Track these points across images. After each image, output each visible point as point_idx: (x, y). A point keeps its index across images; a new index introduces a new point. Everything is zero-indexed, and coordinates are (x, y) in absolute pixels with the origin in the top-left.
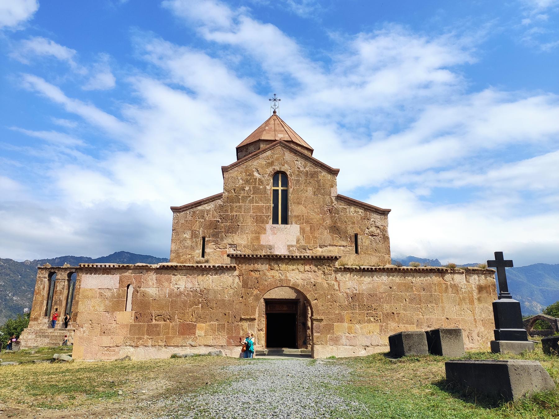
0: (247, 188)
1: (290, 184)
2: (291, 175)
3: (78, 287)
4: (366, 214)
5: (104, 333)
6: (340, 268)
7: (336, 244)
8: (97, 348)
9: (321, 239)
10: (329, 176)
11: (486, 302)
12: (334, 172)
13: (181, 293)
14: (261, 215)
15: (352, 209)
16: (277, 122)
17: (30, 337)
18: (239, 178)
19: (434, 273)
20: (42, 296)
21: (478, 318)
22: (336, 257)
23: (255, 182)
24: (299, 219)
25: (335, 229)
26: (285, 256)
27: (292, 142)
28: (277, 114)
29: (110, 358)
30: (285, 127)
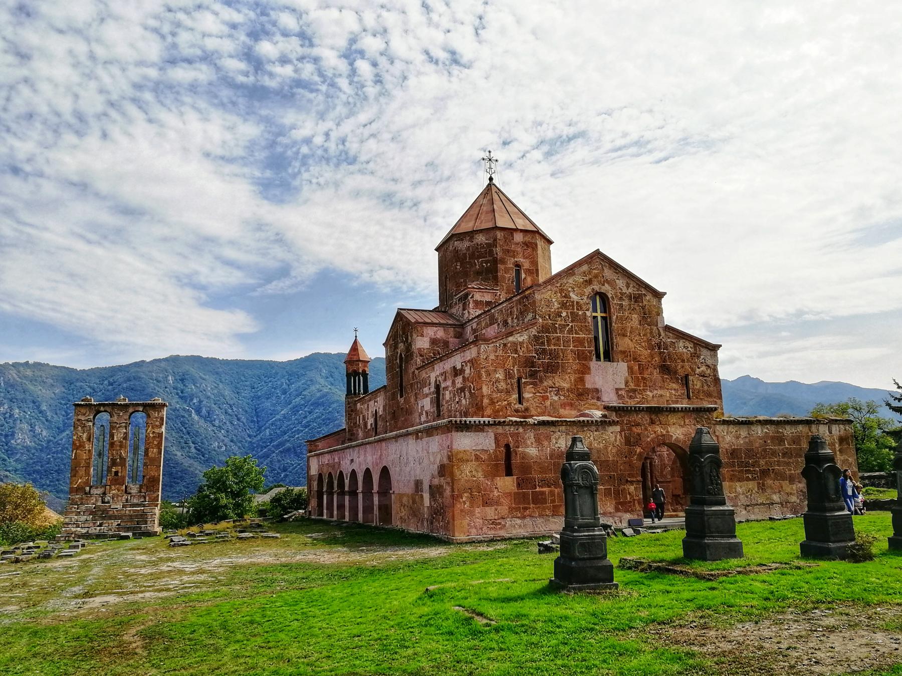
0: (564, 314)
1: (612, 310)
3: (151, 435)
5: (487, 503)
6: (720, 421)
7: (667, 387)
8: (481, 521)
9: (651, 381)
10: (654, 302)
12: (659, 295)
15: (681, 344)
16: (501, 195)
17: (83, 518)
18: (554, 300)
19: (802, 424)
20: (87, 452)
22: (716, 409)
23: (573, 306)
24: (625, 354)
25: (665, 369)
26: (667, 408)
27: (537, 233)
28: (494, 181)
29: (496, 533)
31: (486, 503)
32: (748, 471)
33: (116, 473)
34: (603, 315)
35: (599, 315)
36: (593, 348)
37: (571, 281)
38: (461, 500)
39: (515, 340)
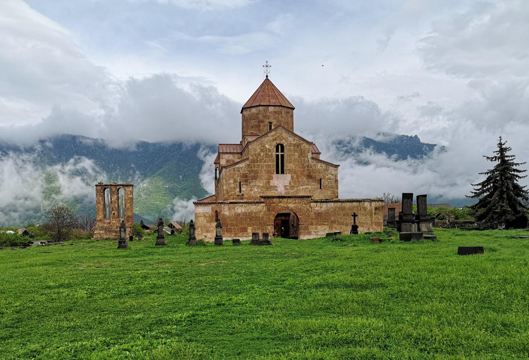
0: (262, 154)
2: (286, 146)
3: (127, 198)
4: (327, 167)
11: (378, 215)
13: (239, 214)
14: (270, 170)
15: (319, 165)
18: (257, 148)
21: (373, 221)
22: (310, 197)
23: (267, 150)
24: (290, 171)
25: (309, 177)
27: (281, 106)
30: (275, 91)
31: (207, 232)
32: (325, 222)
33: (114, 214)
34: (282, 153)
35: (280, 153)
36: (275, 168)
37: (266, 139)
38: (198, 230)
39: (239, 166)
